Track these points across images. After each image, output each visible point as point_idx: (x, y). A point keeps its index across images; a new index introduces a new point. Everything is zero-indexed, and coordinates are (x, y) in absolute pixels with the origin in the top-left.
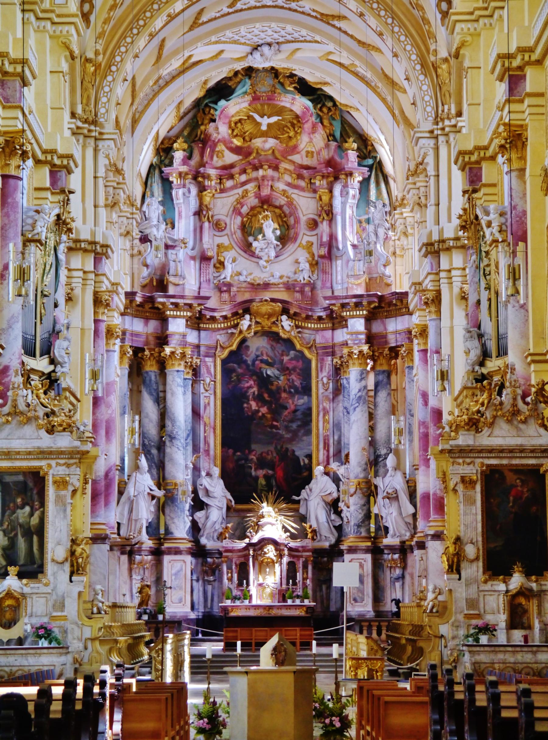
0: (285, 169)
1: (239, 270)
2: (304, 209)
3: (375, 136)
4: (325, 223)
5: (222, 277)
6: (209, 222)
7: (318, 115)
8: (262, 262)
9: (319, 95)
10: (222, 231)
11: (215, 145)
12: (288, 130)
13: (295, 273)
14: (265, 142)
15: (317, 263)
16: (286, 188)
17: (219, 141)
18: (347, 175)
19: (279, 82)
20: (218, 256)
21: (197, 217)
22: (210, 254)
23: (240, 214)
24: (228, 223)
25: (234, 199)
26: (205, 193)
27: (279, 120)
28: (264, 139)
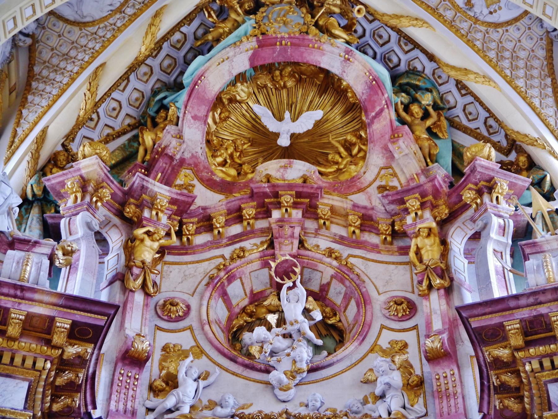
0: (333, 209)
1: (216, 398)
2: (379, 284)
3: (536, 136)
4: (434, 296)
5: (170, 402)
6: (147, 295)
7: (403, 122)
8: (276, 376)
9: (401, 85)
10: (179, 319)
11: (175, 172)
12: (337, 158)
13: (365, 402)
14: (285, 167)
15: (421, 383)
16: (336, 246)
17: (182, 162)
18: (480, 193)
19: (316, 25)
20: (164, 359)
21: (117, 284)
22: (142, 346)
23: (224, 295)
24: (194, 307)
25: (213, 266)
26: (140, 232)
27: (318, 124)
28: (284, 162)
